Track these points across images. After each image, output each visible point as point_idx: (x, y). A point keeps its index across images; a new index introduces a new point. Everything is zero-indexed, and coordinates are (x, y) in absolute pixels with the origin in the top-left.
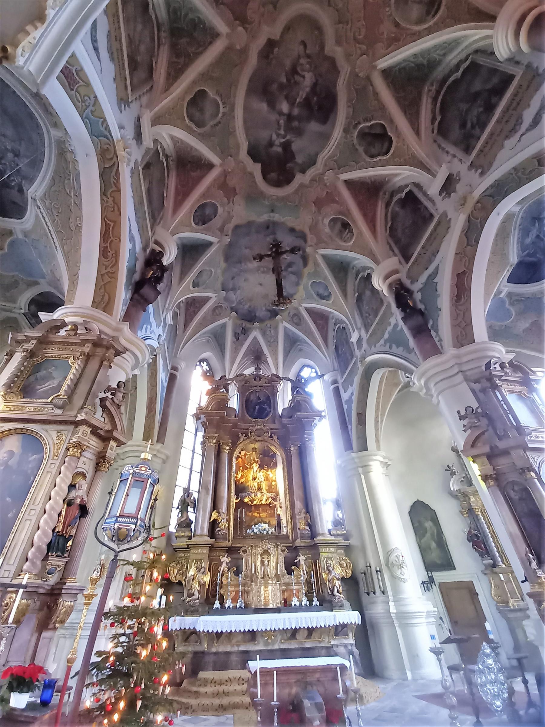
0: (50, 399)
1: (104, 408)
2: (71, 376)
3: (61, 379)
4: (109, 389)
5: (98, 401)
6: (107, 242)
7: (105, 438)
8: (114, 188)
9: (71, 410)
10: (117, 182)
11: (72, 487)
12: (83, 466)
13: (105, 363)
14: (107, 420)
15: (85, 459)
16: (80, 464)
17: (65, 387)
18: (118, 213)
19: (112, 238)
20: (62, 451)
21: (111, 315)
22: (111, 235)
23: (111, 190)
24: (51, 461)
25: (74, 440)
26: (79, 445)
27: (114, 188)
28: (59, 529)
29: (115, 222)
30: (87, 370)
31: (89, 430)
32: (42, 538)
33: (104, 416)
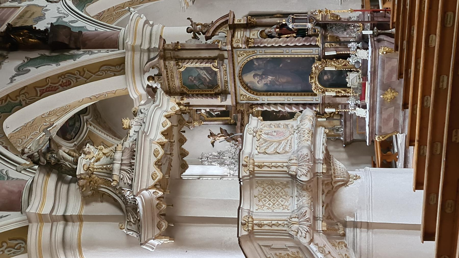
0: (217, 70)
1: (213, 35)
2: (198, 65)
3: (199, 70)
4: (195, 37)
5: (209, 42)
6: (55, 87)
7: (234, 27)
8: (9, 99)
9: (223, 56)
10: (3, 99)
11: (271, 37)
12: (256, 35)
13: (177, 47)
14: (219, 31)
15: (251, 35)
16: (255, 37)
17: (208, 65)
18: (26, 88)
19: (50, 84)
20: (251, 50)
21: (124, 58)
22: (48, 86)
23: (12, 101)
24: (258, 53)
25: (244, 46)
26: (247, 41)
27: (9, 99)
28: (295, 35)
29: (35, 88)
30: (189, 56)
31: (234, 40)
32: (300, 41)
33: (217, 34)
